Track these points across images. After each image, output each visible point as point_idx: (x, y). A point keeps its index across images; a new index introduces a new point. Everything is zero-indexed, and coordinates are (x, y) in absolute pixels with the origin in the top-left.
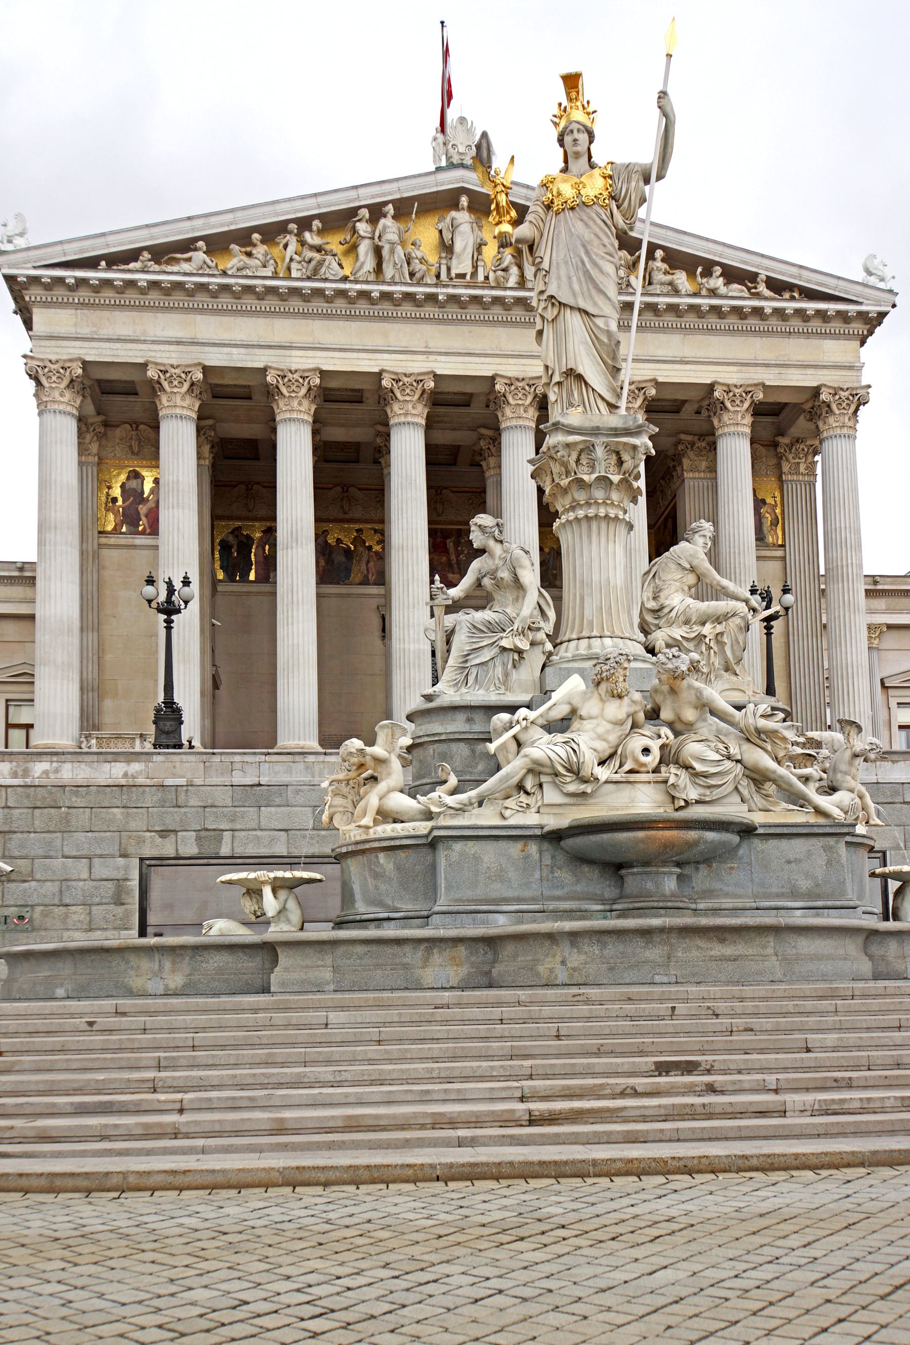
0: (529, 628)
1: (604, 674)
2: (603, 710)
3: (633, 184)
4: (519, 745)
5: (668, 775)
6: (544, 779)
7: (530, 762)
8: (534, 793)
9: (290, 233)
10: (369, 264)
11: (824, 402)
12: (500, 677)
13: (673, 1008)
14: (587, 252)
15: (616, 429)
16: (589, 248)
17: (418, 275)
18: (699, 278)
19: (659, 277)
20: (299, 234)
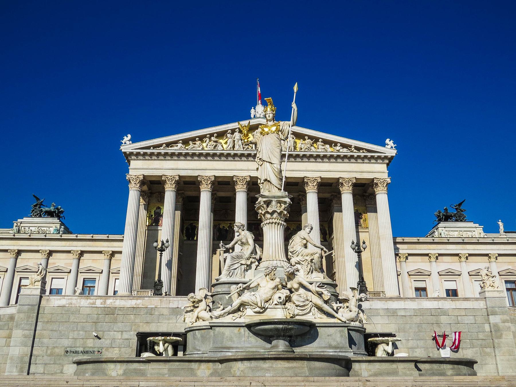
9: (208, 137)
10: (231, 145)
13: (251, 383)
18: (333, 147)
19: (320, 147)
20: (210, 138)
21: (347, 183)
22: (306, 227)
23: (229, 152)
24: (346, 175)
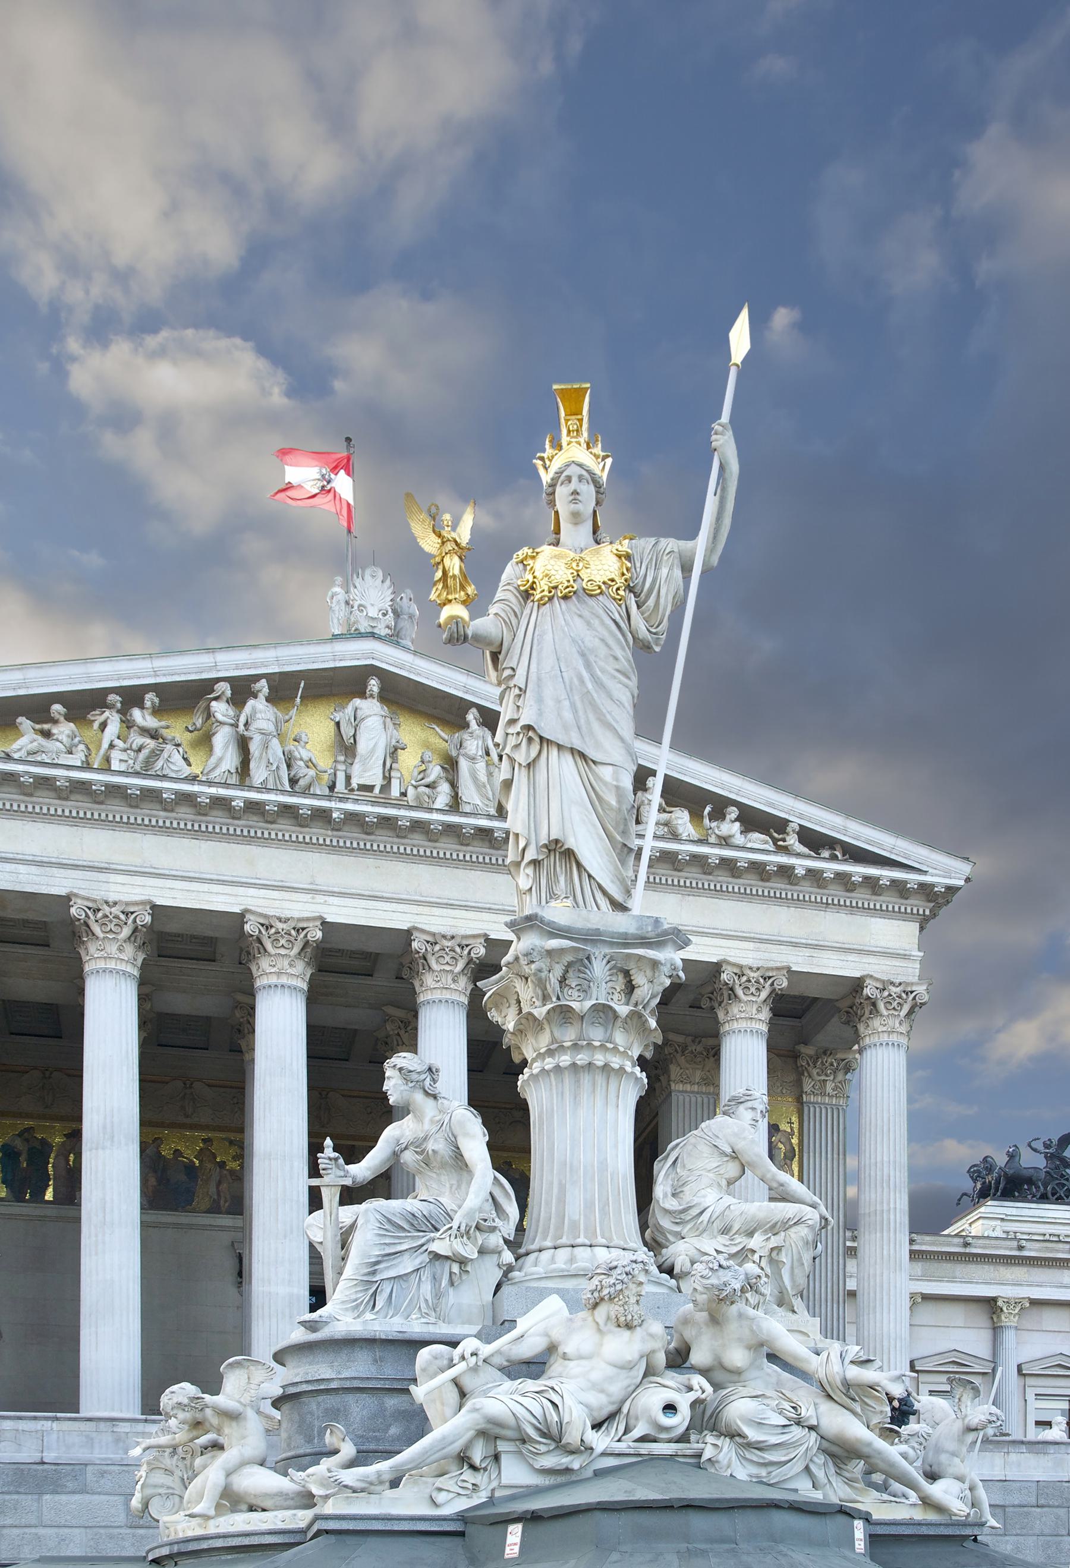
0: (478, 1228)
1: (605, 1292)
2: (601, 1345)
3: (664, 571)
4: (463, 1394)
5: (701, 1446)
6: (502, 1446)
7: (481, 1421)
8: (485, 1469)
11: (868, 998)
12: (429, 1298)
14: (588, 665)
15: (625, 935)
16: (592, 658)
17: (302, 782)
21: (753, 990)
22: (737, 1101)
23: (222, 792)
24: (751, 955)
